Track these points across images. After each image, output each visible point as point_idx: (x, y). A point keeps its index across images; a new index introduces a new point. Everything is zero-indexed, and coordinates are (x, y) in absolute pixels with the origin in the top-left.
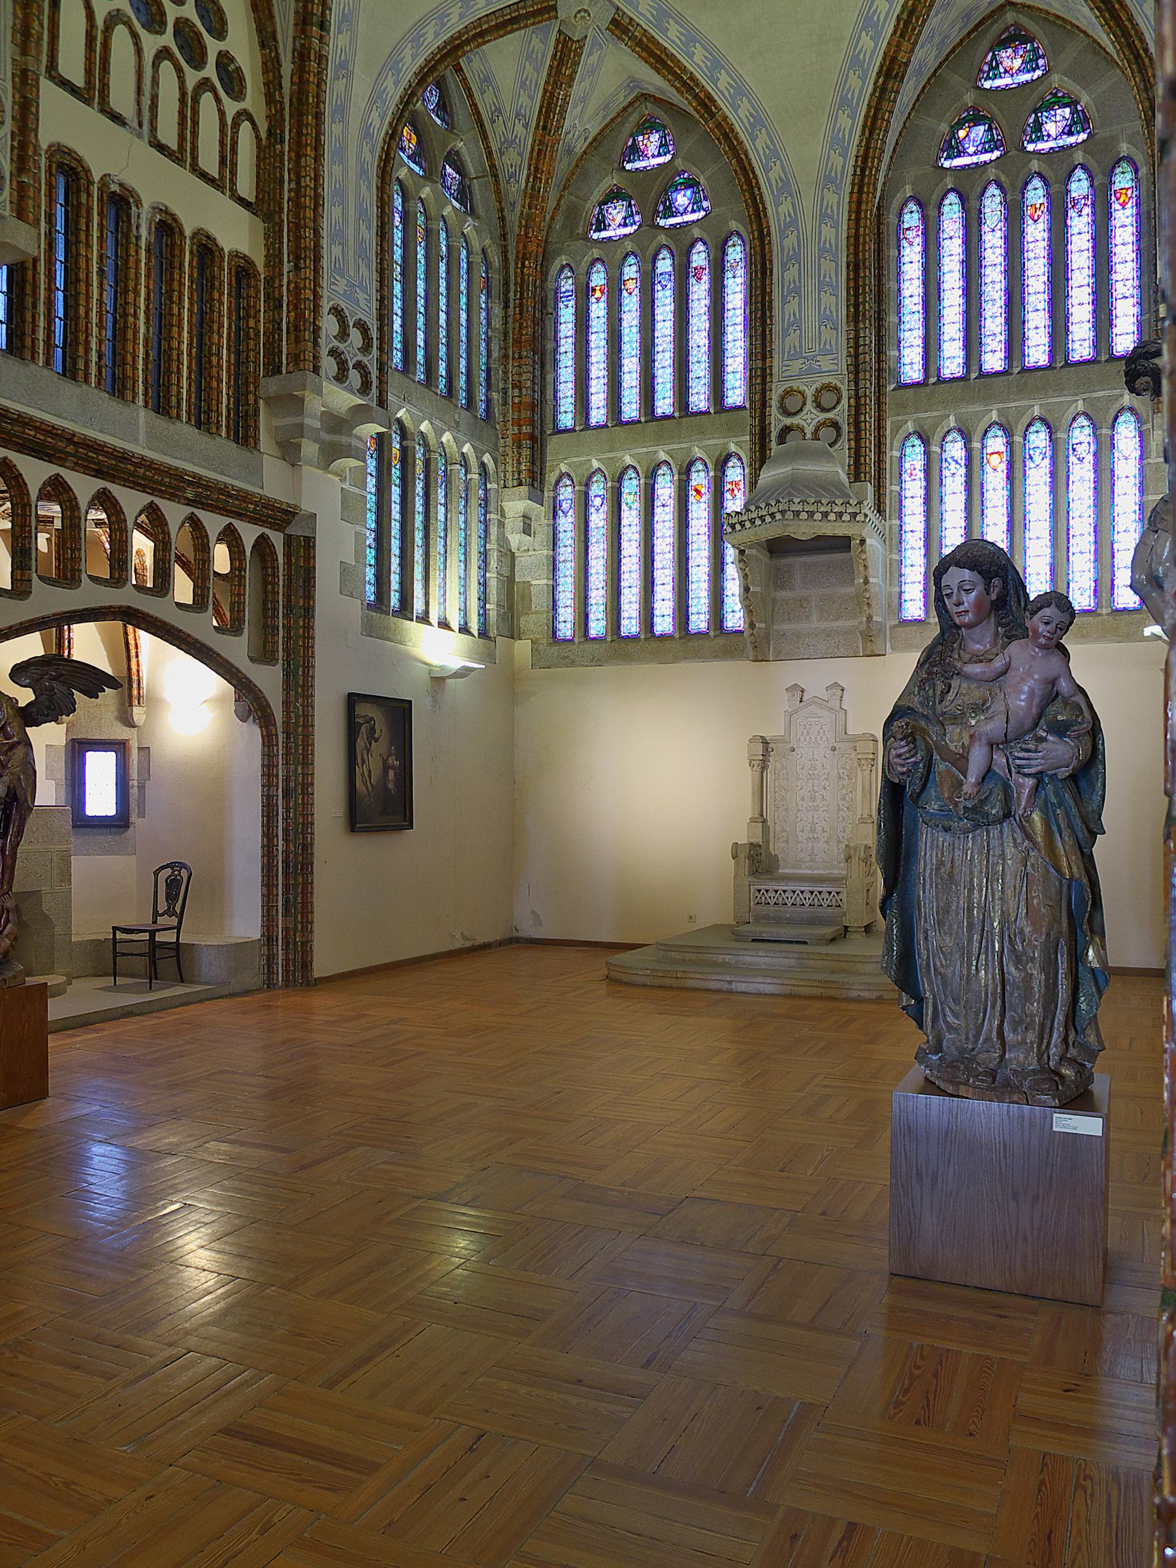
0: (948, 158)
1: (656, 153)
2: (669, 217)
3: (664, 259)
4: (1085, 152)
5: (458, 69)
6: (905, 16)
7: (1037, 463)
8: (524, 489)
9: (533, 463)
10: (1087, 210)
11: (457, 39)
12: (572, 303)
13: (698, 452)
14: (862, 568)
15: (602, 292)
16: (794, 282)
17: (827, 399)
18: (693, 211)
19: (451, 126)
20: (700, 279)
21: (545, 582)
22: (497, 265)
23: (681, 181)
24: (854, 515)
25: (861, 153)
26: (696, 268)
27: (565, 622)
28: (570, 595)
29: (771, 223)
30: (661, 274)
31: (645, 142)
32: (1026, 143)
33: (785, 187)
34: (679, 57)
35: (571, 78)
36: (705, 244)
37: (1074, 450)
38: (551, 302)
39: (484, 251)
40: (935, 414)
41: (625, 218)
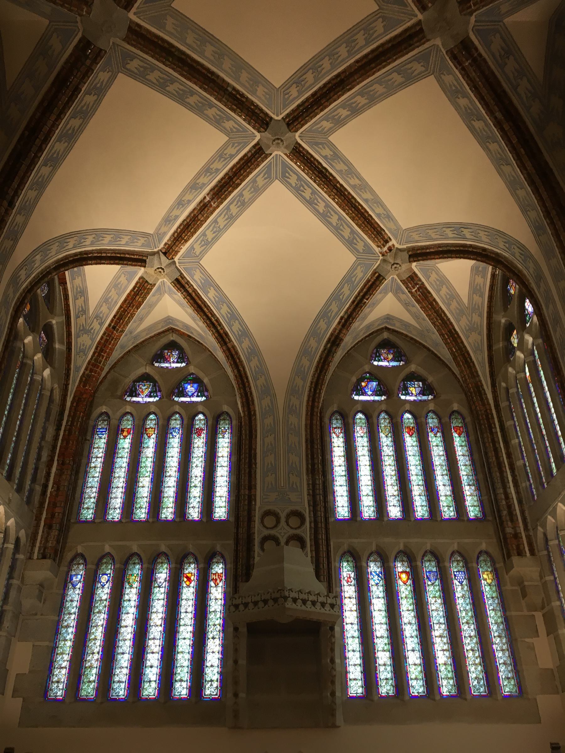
0: (356, 395)
1: (175, 360)
3: (176, 420)
5: (63, 282)
6: (346, 317)
7: (432, 582)
8: (48, 562)
9: (58, 542)
10: (439, 434)
12: (105, 436)
13: (191, 549)
14: (329, 650)
15: (129, 433)
16: (271, 445)
17: (294, 521)
18: (198, 396)
19: (51, 309)
20: (200, 435)
21: (47, 643)
22: (57, 401)
24: (332, 606)
25: (315, 380)
26: (197, 429)
27: (58, 682)
28: (66, 657)
29: (257, 409)
30: (173, 428)
31: (169, 354)
33: (268, 390)
34: (212, 308)
35: (140, 304)
36: (204, 415)
37: (455, 576)
38: (89, 434)
39: (52, 391)
40: (363, 540)
41: (151, 392)
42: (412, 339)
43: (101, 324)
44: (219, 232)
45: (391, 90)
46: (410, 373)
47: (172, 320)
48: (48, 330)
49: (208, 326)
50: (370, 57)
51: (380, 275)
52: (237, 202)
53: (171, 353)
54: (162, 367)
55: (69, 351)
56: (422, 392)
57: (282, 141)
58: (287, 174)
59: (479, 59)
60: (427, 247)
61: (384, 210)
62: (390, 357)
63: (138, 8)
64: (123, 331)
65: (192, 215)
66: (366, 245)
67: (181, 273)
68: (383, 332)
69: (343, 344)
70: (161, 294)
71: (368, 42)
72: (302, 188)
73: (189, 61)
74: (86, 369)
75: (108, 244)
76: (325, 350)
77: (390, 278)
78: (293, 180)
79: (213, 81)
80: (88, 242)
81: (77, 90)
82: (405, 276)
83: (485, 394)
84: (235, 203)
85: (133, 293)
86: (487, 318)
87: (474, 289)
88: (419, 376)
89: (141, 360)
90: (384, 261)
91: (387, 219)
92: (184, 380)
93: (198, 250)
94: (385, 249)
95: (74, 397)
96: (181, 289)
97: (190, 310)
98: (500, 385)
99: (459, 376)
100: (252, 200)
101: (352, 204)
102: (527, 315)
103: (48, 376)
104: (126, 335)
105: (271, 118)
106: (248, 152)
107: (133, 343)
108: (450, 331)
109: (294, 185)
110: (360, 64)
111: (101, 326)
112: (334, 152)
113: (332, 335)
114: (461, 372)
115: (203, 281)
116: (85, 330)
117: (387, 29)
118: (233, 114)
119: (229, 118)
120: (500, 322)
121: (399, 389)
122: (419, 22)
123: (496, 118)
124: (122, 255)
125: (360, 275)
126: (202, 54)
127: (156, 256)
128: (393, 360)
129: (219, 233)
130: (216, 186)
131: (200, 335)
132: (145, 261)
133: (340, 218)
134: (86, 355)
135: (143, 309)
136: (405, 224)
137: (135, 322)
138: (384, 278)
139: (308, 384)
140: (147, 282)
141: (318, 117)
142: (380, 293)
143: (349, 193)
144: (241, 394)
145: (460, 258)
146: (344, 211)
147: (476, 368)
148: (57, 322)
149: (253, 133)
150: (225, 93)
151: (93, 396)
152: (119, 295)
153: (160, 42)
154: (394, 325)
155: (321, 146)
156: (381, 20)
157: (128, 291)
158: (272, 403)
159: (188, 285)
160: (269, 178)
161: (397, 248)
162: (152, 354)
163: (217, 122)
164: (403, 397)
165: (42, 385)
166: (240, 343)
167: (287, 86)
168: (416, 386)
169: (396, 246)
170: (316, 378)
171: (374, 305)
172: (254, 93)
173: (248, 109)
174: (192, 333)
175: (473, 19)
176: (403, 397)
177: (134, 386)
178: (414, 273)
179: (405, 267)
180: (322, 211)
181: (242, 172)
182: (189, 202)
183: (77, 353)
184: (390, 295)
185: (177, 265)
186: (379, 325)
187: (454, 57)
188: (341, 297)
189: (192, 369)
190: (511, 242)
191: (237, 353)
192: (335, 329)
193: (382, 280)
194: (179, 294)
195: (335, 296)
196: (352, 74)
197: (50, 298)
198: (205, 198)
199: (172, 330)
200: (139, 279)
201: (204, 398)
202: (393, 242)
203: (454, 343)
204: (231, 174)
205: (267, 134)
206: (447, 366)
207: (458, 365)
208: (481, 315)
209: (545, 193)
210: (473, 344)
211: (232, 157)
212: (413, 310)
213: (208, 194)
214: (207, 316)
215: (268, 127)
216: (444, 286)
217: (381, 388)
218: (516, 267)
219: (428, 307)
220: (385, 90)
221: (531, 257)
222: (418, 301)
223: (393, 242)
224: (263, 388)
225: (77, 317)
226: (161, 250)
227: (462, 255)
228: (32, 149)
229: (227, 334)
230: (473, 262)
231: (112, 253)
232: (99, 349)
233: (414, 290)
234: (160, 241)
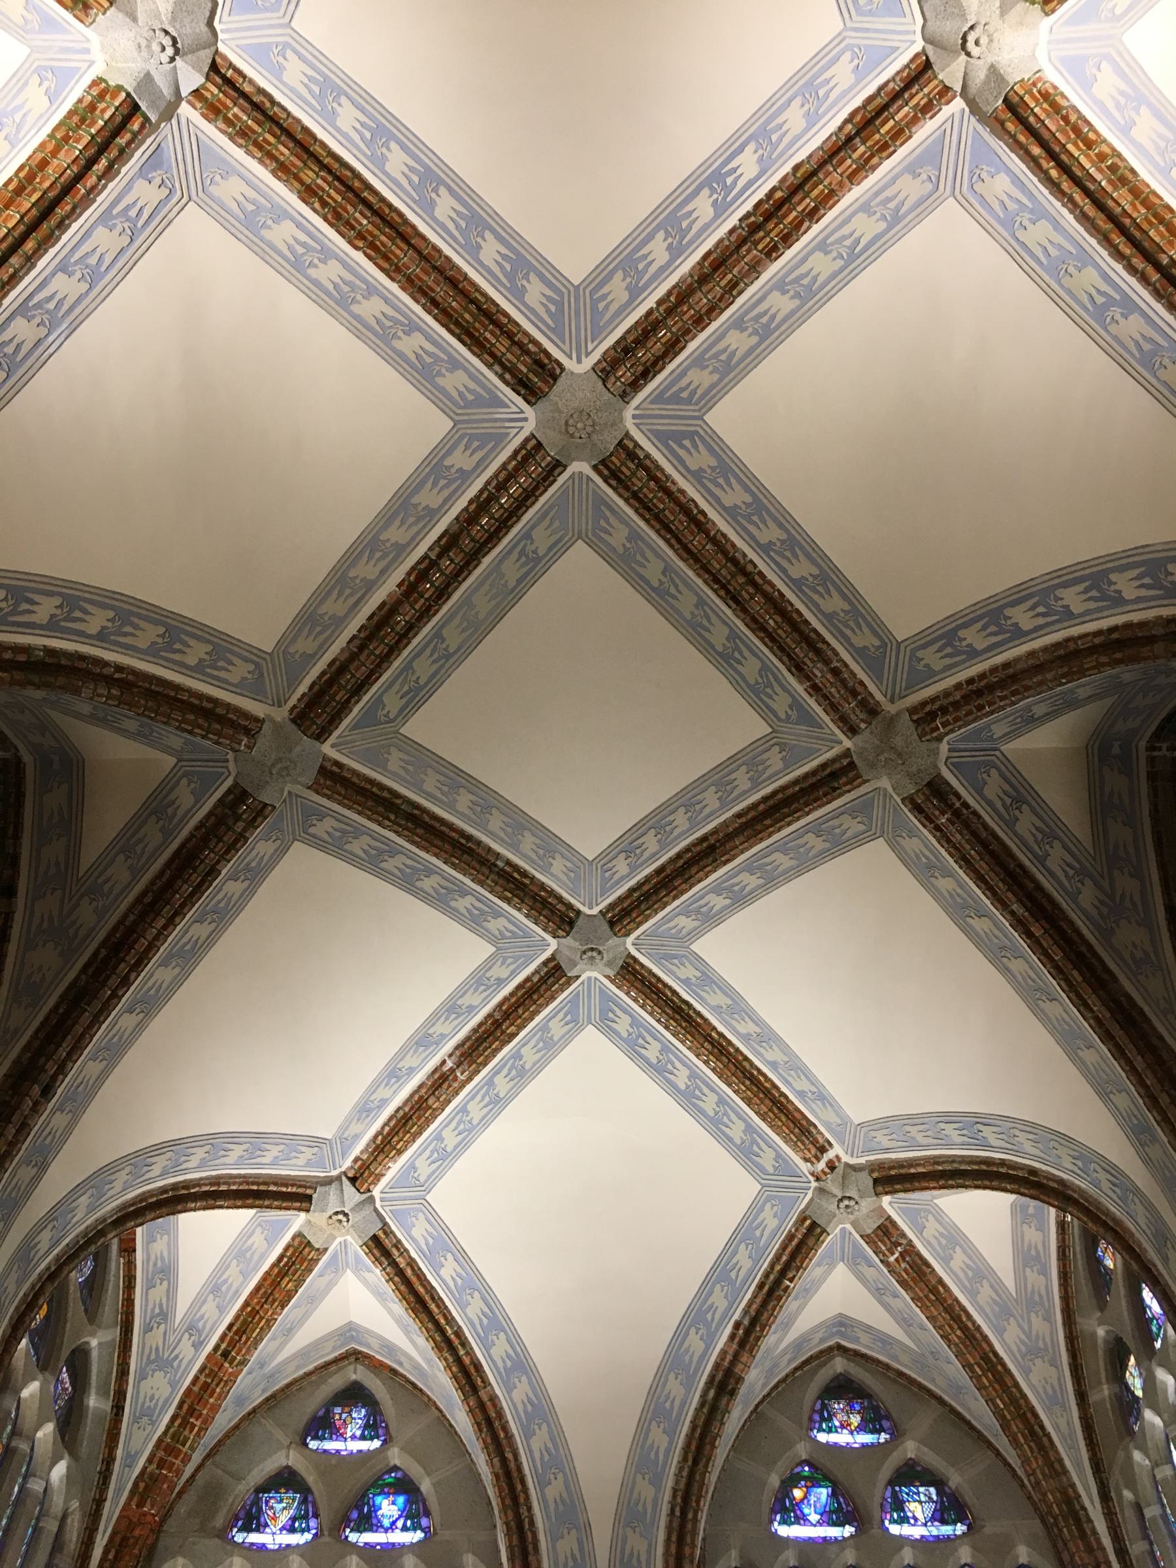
0: (784, 1522)
1: (358, 1433)
2: (365, 1530)
4: (974, 1548)
5: (128, 1249)
6: (746, 1322)
11: (184, 1188)
18: (405, 1529)
22: (73, 1547)
23: (390, 1480)
25: (682, 1486)
31: (344, 1416)
32: (887, 1523)
35: (290, 1296)
41: (294, 1519)
42: (901, 1374)
43: (198, 1346)
44: (470, 1131)
45: (804, 865)
46: (906, 1464)
47: (355, 1330)
48: (78, 1362)
49: (438, 1348)
50: (762, 807)
51: (814, 1225)
52: (510, 1071)
53: (350, 1413)
54: (325, 1451)
55: (117, 1415)
56: (938, 1515)
57: (600, 953)
58: (611, 1015)
59: (965, 811)
60: (911, 1163)
61: (812, 1084)
62: (855, 1420)
63: (339, 737)
64: (244, 1363)
65: (416, 1097)
66: (779, 1156)
67: (385, 1224)
68: (833, 1357)
69: (743, 1390)
70: (337, 1270)
71: (756, 785)
72: (641, 1041)
73: (427, 819)
74: (150, 1460)
75: (236, 1164)
76: (702, 1404)
77: (837, 1230)
78: (623, 1025)
79: (470, 852)
80: (194, 1162)
81: (212, 872)
82: (870, 1227)
83: (1090, 1521)
84: (505, 1071)
85: (276, 1270)
86: (1064, 1324)
87: (1025, 1257)
88: (927, 1471)
89: (280, 1435)
90: (821, 1191)
91: (819, 1103)
92: (374, 1485)
93: (424, 1169)
94: (822, 1165)
95: (114, 1533)
96: (383, 1259)
97: (399, 1308)
98: (1120, 1496)
99: (1020, 1472)
100: (540, 1066)
101: (744, 1071)
102: (1151, 1320)
103: (61, 1480)
104: (249, 1373)
105: (578, 912)
106: (533, 974)
107: (264, 1391)
108: (985, 1357)
109: (625, 1035)
110: (744, 820)
111: (196, 1351)
112: (703, 973)
113: (717, 1366)
114: (1025, 1462)
115: (431, 1241)
116: (161, 1362)
117: (788, 765)
118: (505, 906)
119: (497, 914)
120: (1094, 1335)
121: (882, 1505)
122: (847, 753)
123: (1013, 913)
124: (262, 1188)
125: (772, 1223)
126: (451, 807)
127: (333, 1185)
128: (861, 1428)
129: (469, 1133)
130: (468, 1038)
131: (417, 1367)
132: (309, 1198)
133: (721, 1101)
134: (153, 1423)
135: (295, 1307)
136: (857, 1115)
137: (273, 1339)
138: (824, 1231)
139: (667, 1496)
140: (309, 1242)
141: (668, 909)
142: (819, 1265)
143: (737, 1050)
144: (507, 1524)
145: (985, 1188)
146: (729, 1085)
147: (1057, 1452)
148: (100, 1344)
149: (544, 940)
150: (491, 871)
151: (158, 1530)
152: (246, 1275)
153: (374, 790)
154: (857, 1340)
155: (676, 961)
156: (777, 748)
157: (266, 1267)
158: (581, 1550)
159: (398, 1250)
160: (575, 1025)
161: (847, 1165)
162: (305, 1419)
163: (475, 922)
164: (894, 1529)
165: (42, 1504)
166: (509, 1389)
167: (607, 857)
168: (923, 1498)
169: (843, 1160)
170: (684, 1480)
171: (808, 1292)
172: (546, 869)
173: (535, 897)
174: (401, 1364)
175: (944, 747)
176: (894, 1529)
177: (257, 1502)
178: (889, 1218)
179: (867, 1205)
180: (683, 1087)
181: (520, 1011)
182: (411, 1071)
183: (136, 1420)
184: (841, 1270)
185: (378, 1204)
186: (822, 1340)
187: (917, 809)
188: (733, 1274)
189: (395, 1456)
190: (1086, 1157)
191: (500, 1414)
192: (723, 1353)
193: (821, 1234)
194: (378, 1271)
195: (720, 1272)
196: (729, 837)
197: (93, 1287)
198: (444, 1062)
199: (355, 1356)
200: (293, 1238)
201: (419, 1535)
202: (836, 1151)
203: (997, 1386)
204: (497, 1016)
205: (569, 941)
206: (990, 1445)
207: (1014, 1442)
208: (1048, 1318)
209: (1139, 1058)
210: (1041, 1391)
211: (501, 982)
212: (896, 1304)
213: (450, 1056)
214: (436, 1323)
215: (572, 928)
216: (958, 1249)
217: (839, 1503)
218: (1108, 1213)
219: (927, 1297)
220: (794, 863)
221: (1137, 1191)
222: (903, 1283)
223: (836, 1151)
224: (561, 1508)
225: (147, 1329)
226: (345, 1173)
227: (987, 1183)
228: (109, 983)
229: (478, 1367)
230: (1012, 1197)
231: (241, 1184)
232: (186, 1407)
233: (892, 1259)
234: (344, 1155)
